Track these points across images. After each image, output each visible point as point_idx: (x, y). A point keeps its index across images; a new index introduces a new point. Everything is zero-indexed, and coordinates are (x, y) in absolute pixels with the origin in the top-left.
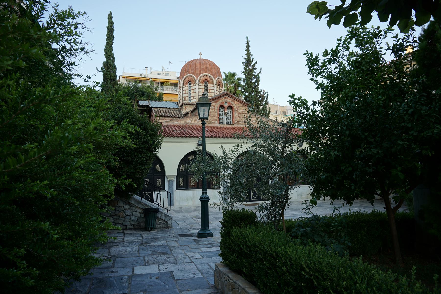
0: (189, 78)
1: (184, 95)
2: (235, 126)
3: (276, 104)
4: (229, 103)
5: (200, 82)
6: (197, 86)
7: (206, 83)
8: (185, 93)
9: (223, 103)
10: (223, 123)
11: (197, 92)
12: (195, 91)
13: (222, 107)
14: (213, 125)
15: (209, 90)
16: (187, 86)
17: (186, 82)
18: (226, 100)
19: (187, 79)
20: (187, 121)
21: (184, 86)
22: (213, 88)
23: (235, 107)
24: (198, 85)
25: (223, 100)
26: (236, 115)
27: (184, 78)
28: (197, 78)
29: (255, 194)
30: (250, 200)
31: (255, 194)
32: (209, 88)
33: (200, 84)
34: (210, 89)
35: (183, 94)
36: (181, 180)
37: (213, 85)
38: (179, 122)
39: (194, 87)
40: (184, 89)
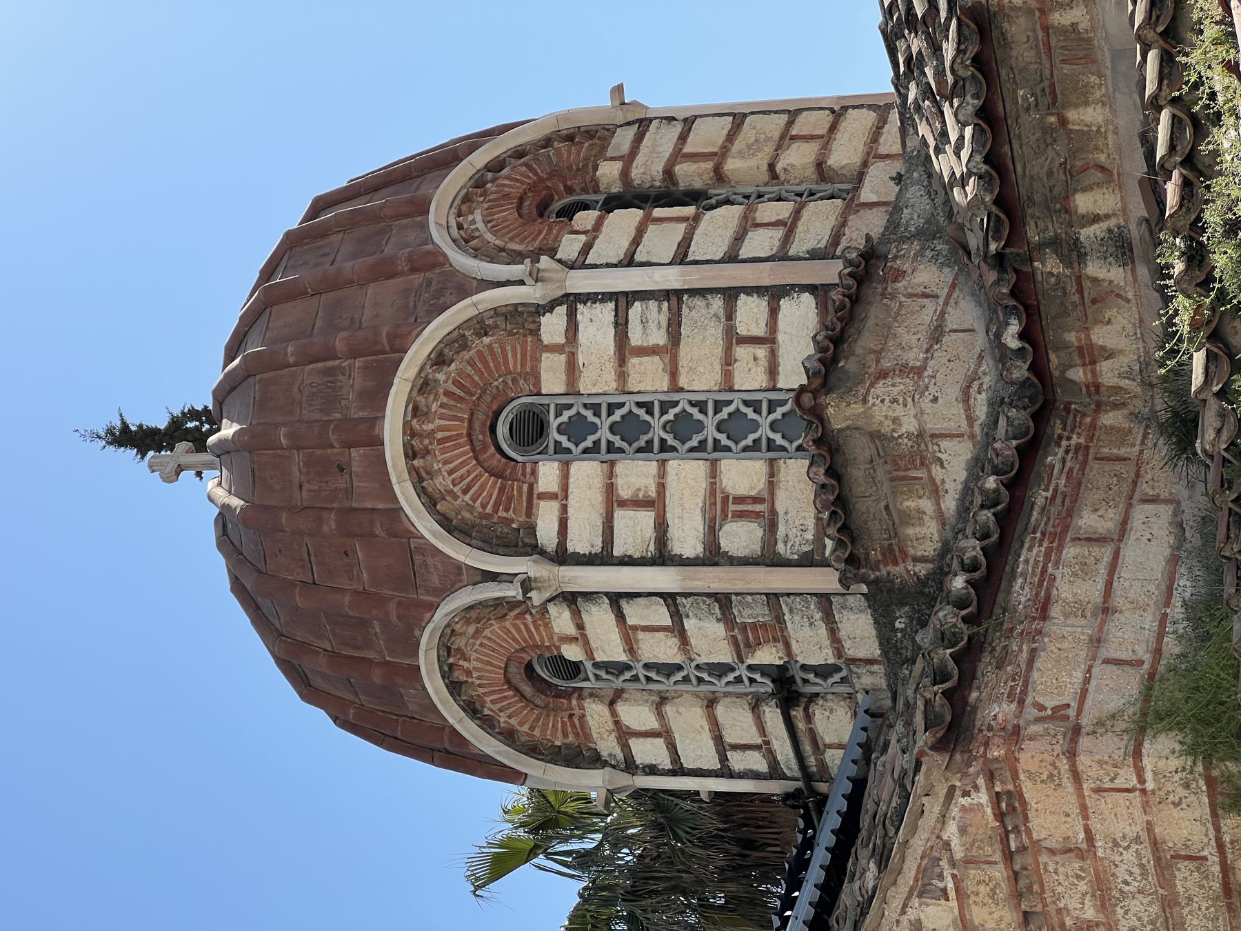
1: (687, 538)
6: (580, 282)
8: (656, 503)
11: (672, 278)
12: (648, 325)
16: (548, 474)
17: (478, 496)
19: (452, 468)
21: (547, 532)
27: (426, 526)
34: (678, 155)
35: (662, 557)
40: (583, 539)
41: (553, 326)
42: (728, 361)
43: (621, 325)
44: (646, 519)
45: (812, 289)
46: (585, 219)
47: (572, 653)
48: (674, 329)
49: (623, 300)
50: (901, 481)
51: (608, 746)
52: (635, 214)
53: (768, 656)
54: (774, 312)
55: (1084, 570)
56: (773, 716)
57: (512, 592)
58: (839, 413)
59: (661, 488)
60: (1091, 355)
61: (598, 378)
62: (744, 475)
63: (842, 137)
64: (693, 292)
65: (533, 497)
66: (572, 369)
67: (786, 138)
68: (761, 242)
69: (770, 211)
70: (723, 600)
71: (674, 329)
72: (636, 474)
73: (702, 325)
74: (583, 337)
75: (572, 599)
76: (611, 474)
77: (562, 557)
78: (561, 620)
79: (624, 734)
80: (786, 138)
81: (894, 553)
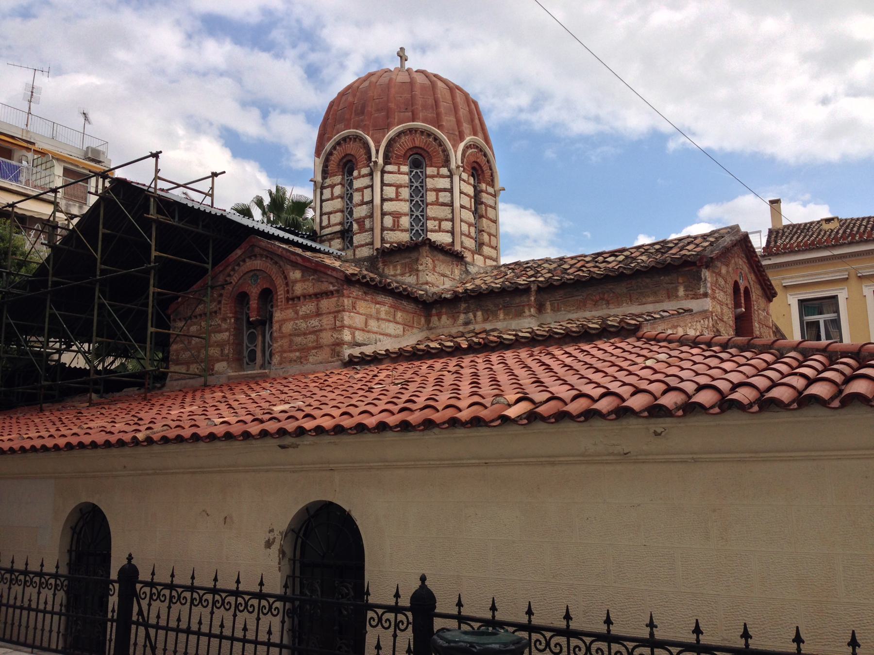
1: (388, 206)
6: (456, 179)
8: (397, 199)
11: (457, 204)
12: (444, 197)
16: (405, 169)
19: (406, 142)
21: (389, 168)
28: (455, 146)
34: (486, 206)
35: (383, 200)
40: (388, 178)
41: (444, 171)
42: (435, 219)
43: (445, 190)
44: (393, 196)
45: (453, 242)
46: (472, 181)
47: (355, 173)
49: (451, 191)
50: (404, 266)
51: (328, 182)
52: (472, 194)
53: (355, 227)
54: (447, 232)
55: (387, 313)
56: (338, 228)
57: (373, 159)
58: (425, 250)
59: (401, 200)
60: (439, 316)
61: (430, 183)
62: (405, 221)
63: (490, 249)
64: (453, 210)
65: (399, 164)
66: (432, 177)
67: (490, 235)
68: (465, 227)
69: (472, 230)
70: (371, 216)
72: (405, 193)
73: (445, 212)
74: (441, 179)
75: (371, 174)
76: (405, 187)
78: (365, 171)
79: (332, 186)
80: (490, 235)
81: (385, 264)
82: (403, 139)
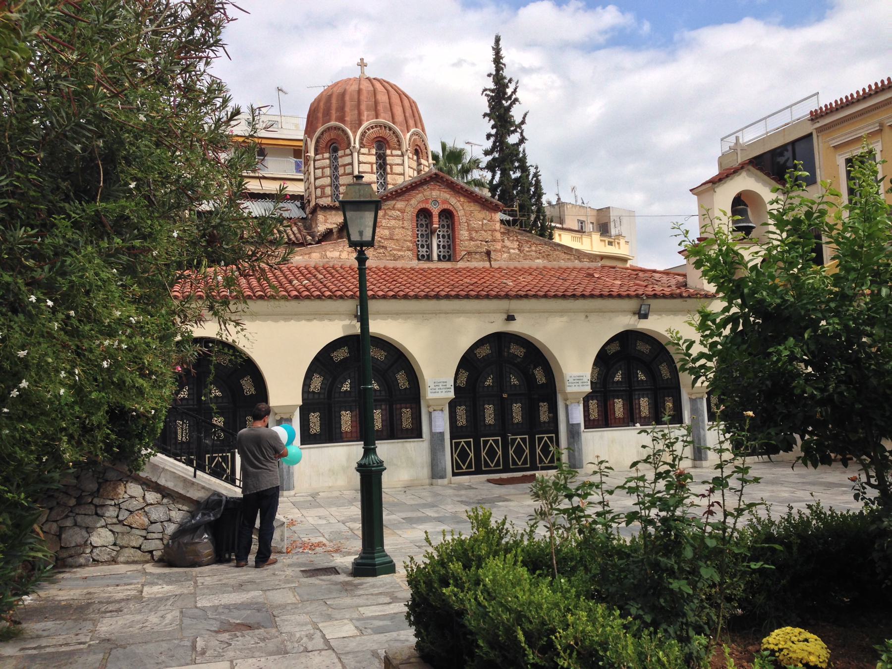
0: (333, 135)
1: (318, 183)
2: (460, 265)
3: (579, 203)
4: (445, 201)
5: (362, 145)
6: (355, 155)
7: (379, 148)
8: (323, 177)
9: (426, 201)
10: (429, 258)
13: (424, 214)
14: (399, 264)
15: (388, 167)
16: (327, 155)
17: (323, 144)
18: (435, 193)
19: (326, 137)
20: (329, 254)
21: (318, 157)
22: (398, 160)
23: (461, 213)
24: (359, 153)
25: (427, 193)
26: (463, 234)
28: (355, 133)
29: (519, 451)
30: (506, 470)
31: (519, 451)
32: (389, 160)
33: (363, 150)
34: (391, 165)
35: (315, 179)
36: (315, 419)
37: (399, 153)
38: (306, 257)
39: (347, 160)
40: (318, 164)
43: (348, 164)
48: (349, 174)
62: (328, 191)
65: (322, 153)
66: (341, 157)
71: (349, 174)
72: (328, 171)
77: (315, 161)
82: (325, 136)
